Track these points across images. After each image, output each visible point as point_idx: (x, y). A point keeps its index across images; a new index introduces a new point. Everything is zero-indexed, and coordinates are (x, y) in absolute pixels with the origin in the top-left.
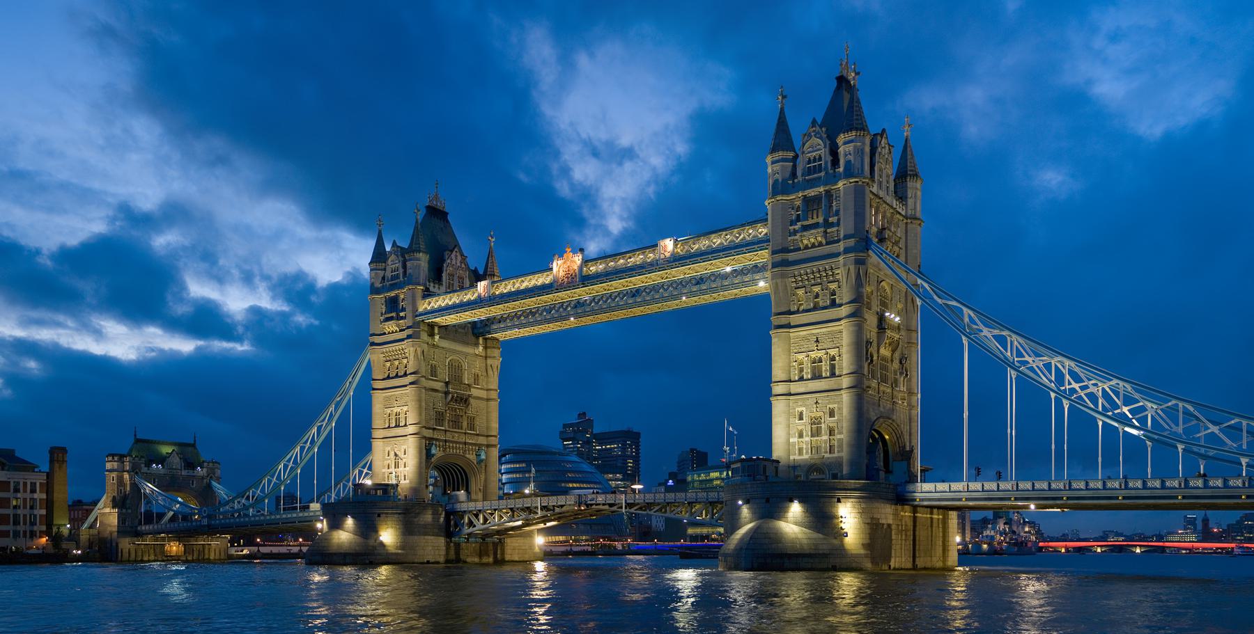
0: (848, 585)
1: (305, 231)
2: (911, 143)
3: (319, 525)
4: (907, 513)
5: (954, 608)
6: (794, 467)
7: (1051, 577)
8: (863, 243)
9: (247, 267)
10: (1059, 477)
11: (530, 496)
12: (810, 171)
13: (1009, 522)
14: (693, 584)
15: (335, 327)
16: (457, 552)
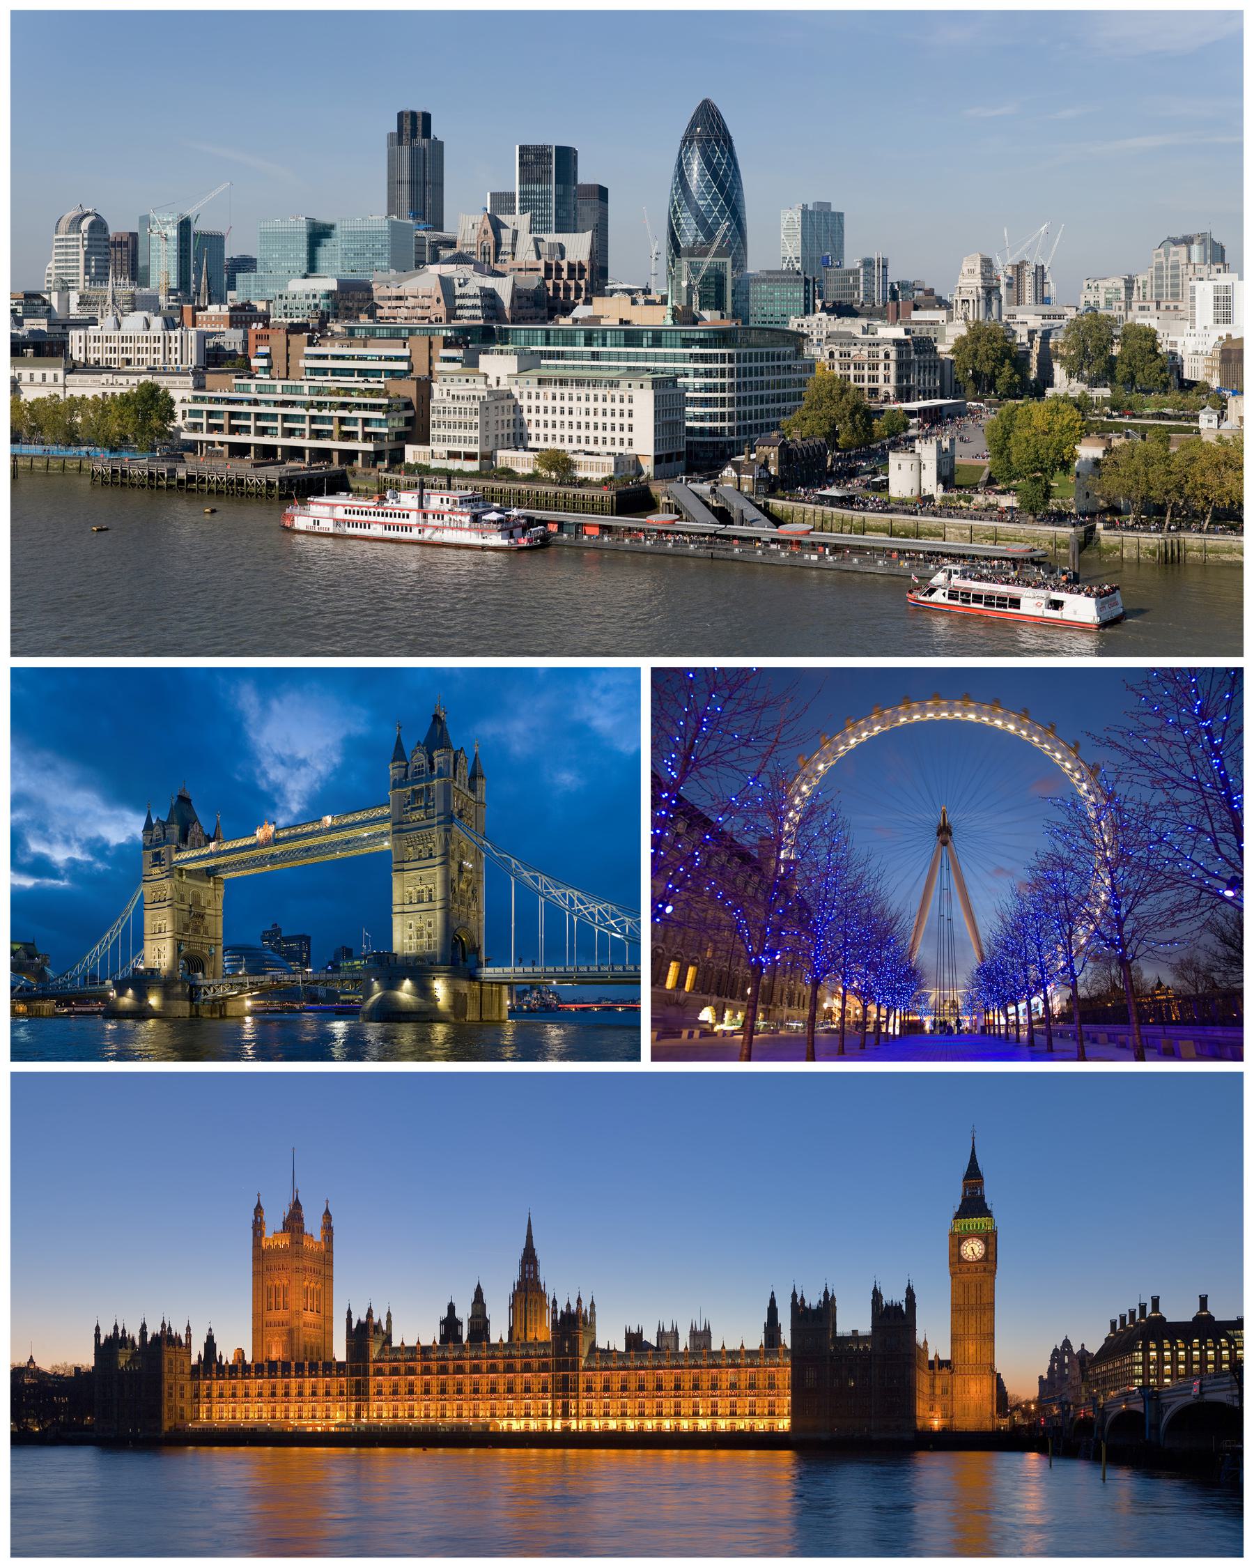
0: (440, 1031)
1: (102, 811)
2: (479, 756)
3: (111, 994)
4: (476, 986)
5: (506, 1045)
6: (406, 958)
7: (566, 1025)
8: (449, 819)
9: (66, 833)
10: (571, 964)
11: (242, 976)
12: (416, 774)
13: (540, 992)
14: (343, 1030)
15: (121, 871)
16: (197, 1011)
